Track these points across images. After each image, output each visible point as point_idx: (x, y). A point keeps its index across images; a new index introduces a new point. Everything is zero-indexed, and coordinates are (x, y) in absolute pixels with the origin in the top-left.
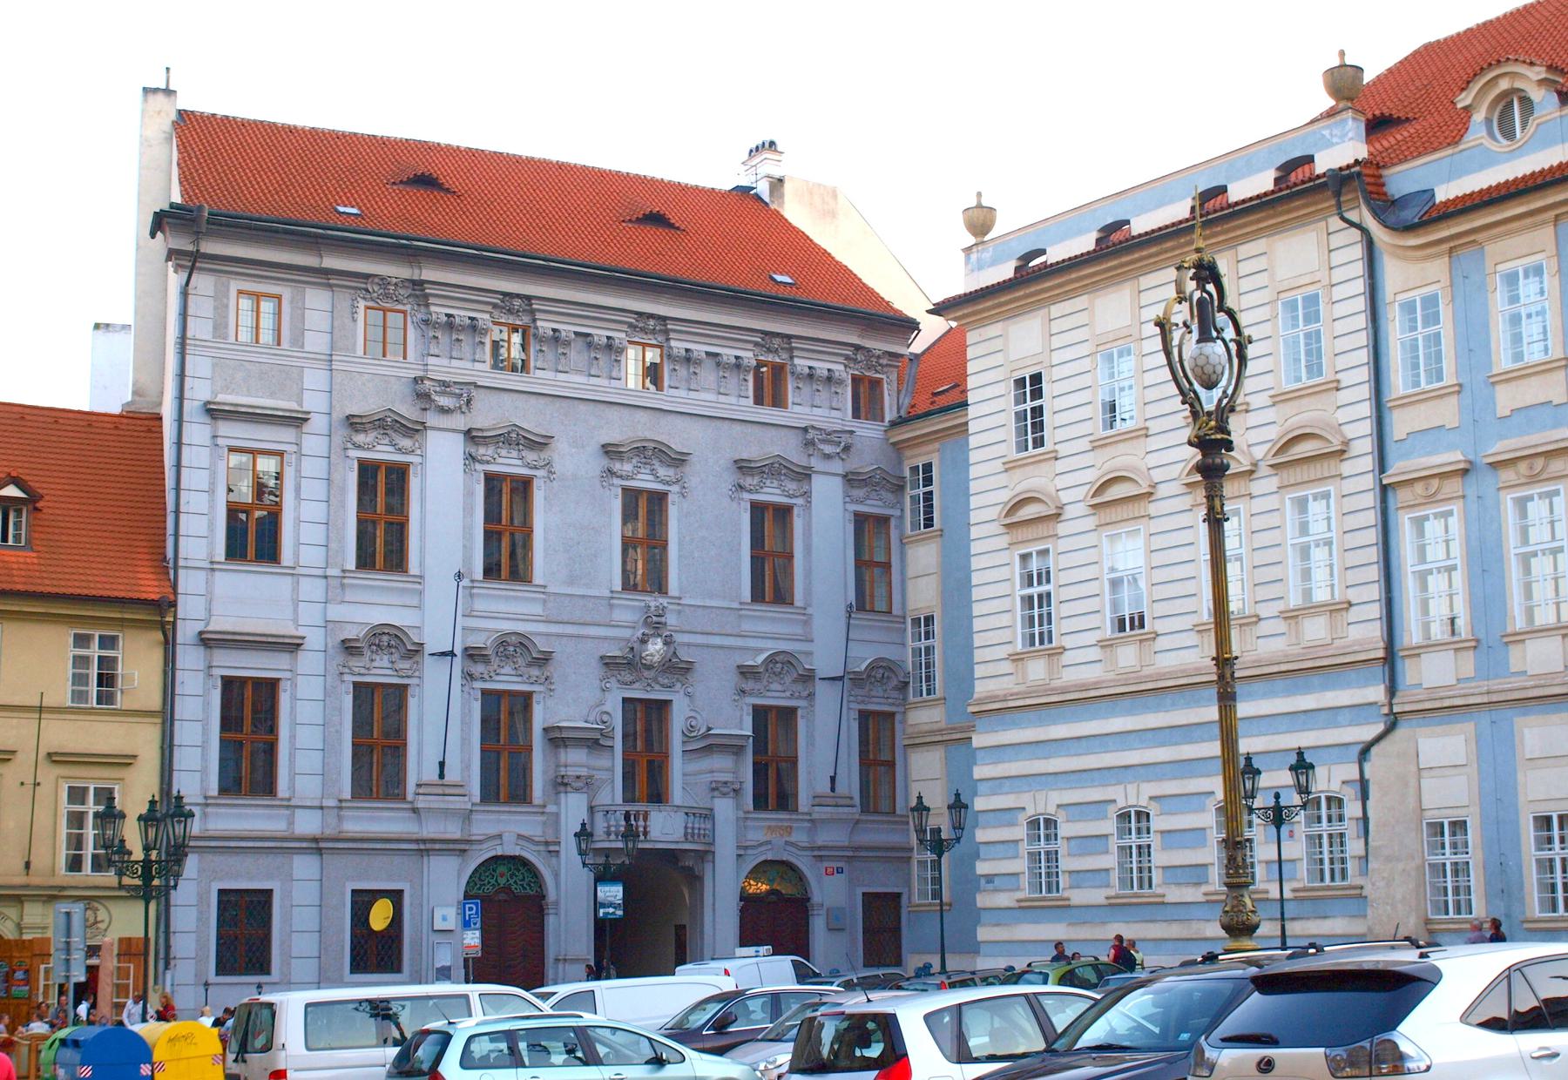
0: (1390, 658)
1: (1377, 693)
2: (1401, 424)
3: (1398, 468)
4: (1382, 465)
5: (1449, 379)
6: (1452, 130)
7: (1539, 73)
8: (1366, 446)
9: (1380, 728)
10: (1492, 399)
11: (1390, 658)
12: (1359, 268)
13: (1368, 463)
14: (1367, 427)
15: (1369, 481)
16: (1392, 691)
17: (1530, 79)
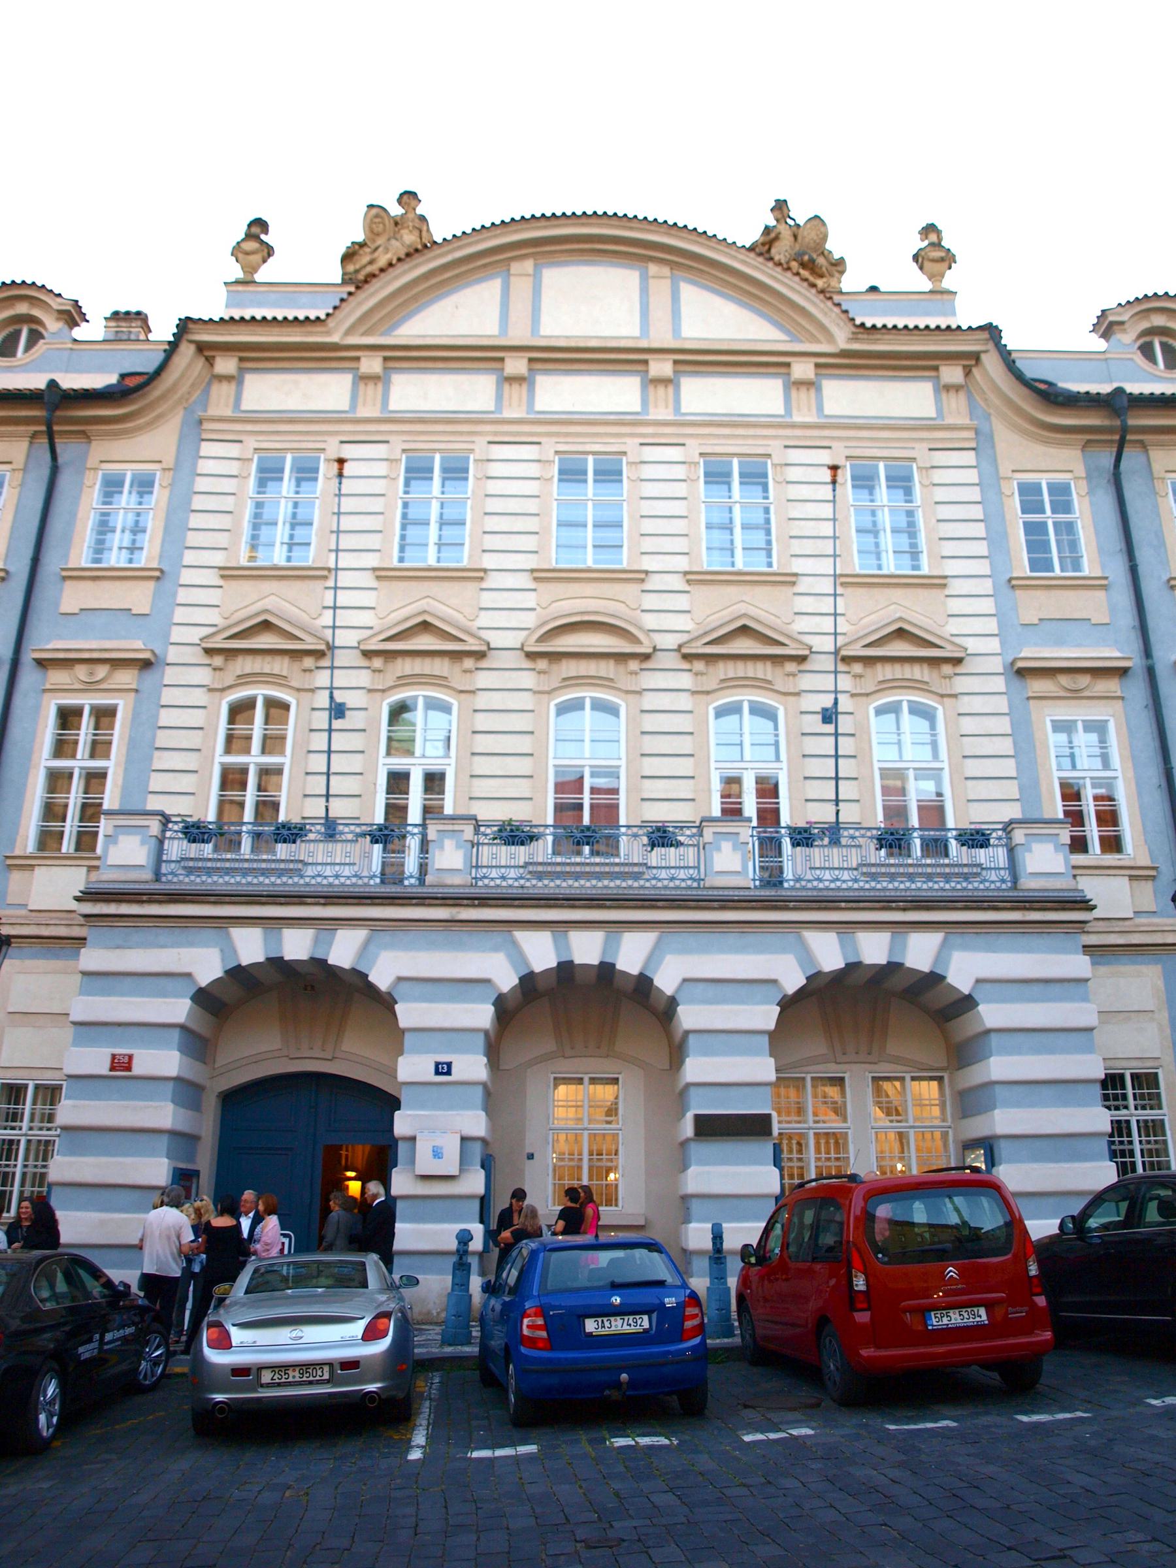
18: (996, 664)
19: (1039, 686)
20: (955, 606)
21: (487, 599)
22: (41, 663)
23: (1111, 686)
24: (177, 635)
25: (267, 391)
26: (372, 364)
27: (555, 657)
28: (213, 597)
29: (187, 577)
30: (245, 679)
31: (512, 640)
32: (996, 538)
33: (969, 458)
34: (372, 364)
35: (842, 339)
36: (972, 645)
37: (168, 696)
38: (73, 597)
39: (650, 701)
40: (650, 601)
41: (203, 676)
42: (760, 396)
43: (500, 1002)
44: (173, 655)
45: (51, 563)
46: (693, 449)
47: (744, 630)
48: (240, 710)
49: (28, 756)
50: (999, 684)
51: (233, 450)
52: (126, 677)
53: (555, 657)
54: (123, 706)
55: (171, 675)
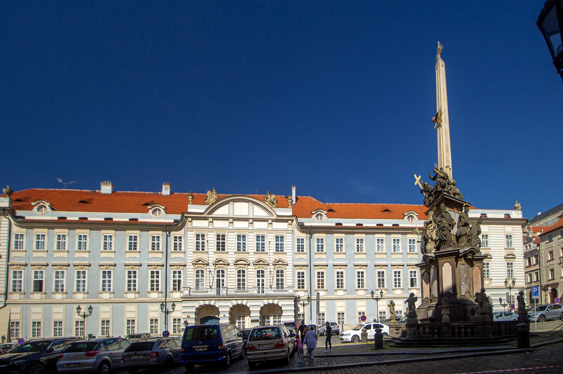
0: (6, 294)
1: (3, 299)
2: (13, 254)
3: (11, 262)
4: (8, 261)
5: (24, 249)
6: (30, 208)
7: (49, 204)
8: (5, 257)
9: (3, 305)
10: (32, 254)
11: (6, 294)
12: (7, 226)
13: (5, 260)
14: (5, 254)
15: (5, 263)
16: (6, 299)
17: (47, 205)
18: (291, 265)
19: (296, 267)
20: (287, 257)
21: (228, 256)
22: (170, 266)
23: (305, 267)
24: (188, 261)
25: (196, 223)
26: (211, 220)
27: (237, 265)
28: (192, 255)
29: (188, 253)
30: (198, 267)
31: (232, 262)
32: (293, 247)
33: (291, 235)
34: (211, 220)
35: (275, 217)
36: (288, 262)
37: (188, 270)
38: (173, 255)
39: (249, 270)
40: (249, 256)
41: (192, 267)
42: (264, 225)
43: (230, 308)
44: (188, 264)
45: (169, 251)
46: (255, 234)
47: (261, 261)
48: (198, 272)
49: (170, 278)
50: (291, 267)
51: (192, 233)
52: (182, 267)
53: (237, 265)
54: (182, 271)
55: (187, 267)
